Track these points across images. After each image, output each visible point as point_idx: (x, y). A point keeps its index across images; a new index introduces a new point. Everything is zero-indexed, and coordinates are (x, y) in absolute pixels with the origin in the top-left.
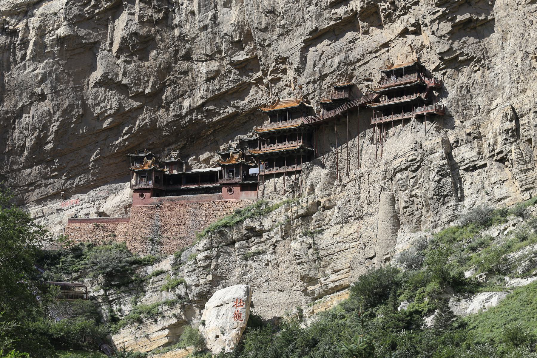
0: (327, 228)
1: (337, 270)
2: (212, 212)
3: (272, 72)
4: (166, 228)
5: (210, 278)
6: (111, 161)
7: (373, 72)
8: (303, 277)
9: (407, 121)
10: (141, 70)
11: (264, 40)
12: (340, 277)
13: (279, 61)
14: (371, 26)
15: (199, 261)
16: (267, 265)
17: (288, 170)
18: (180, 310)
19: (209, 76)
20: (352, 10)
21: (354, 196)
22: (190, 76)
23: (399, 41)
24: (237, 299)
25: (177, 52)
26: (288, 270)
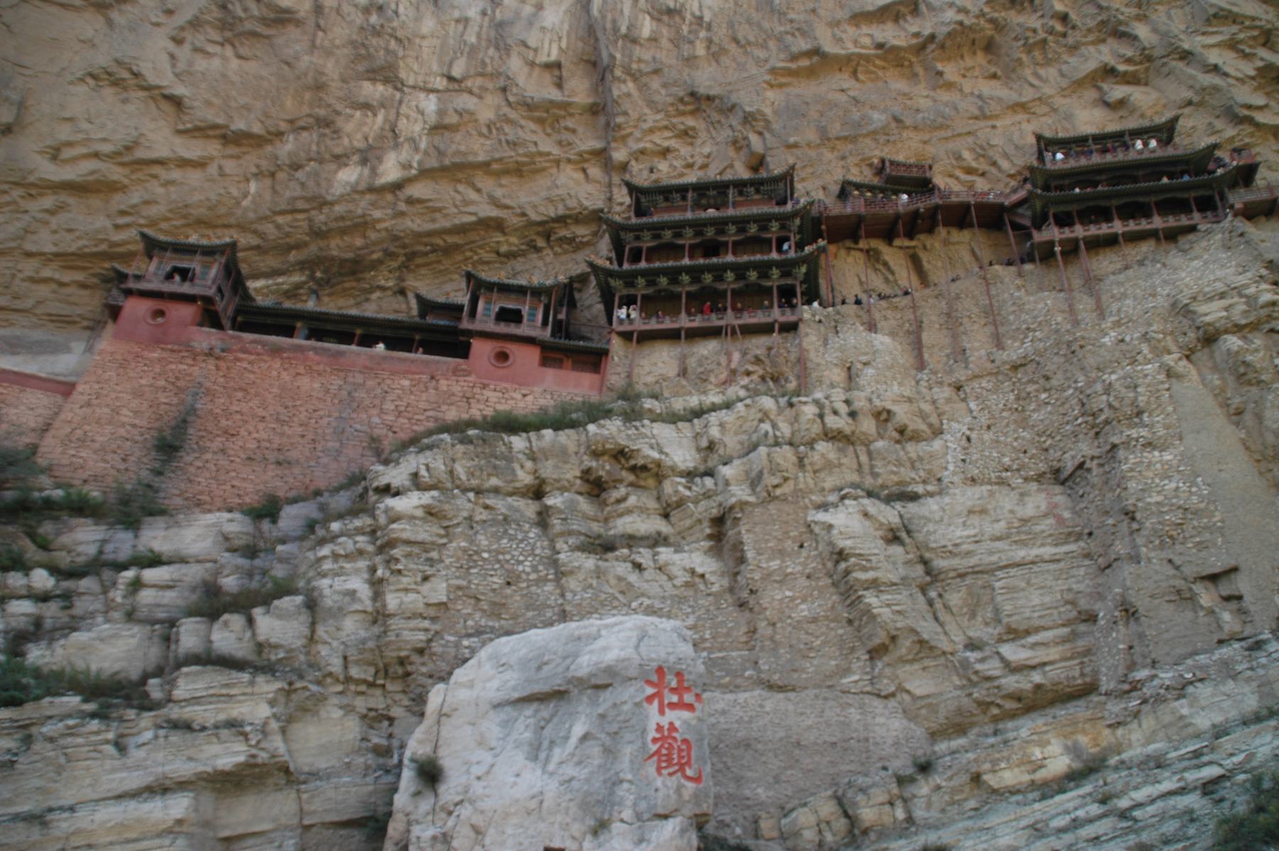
0: (931, 495)
1: (1022, 627)
2: (422, 405)
3: (651, 131)
4: (224, 423)
5: (438, 590)
6: (46, 273)
7: (991, 153)
8: (893, 638)
9: (1172, 236)
10: (236, 78)
11: (640, 61)
12: (1041, 655)
13: (681, 107)
14: (964, 76)
15: (395, 519)
16: (687, 585)
17: (737, 322)
18: (264, 711)
19: (447, 121)
20: (917, 35)
21: (1004, 414)
22: (380, 118)
23: (1068, 100)
24: (660, 671)
25: (358, 58)
26: (804, 610)
